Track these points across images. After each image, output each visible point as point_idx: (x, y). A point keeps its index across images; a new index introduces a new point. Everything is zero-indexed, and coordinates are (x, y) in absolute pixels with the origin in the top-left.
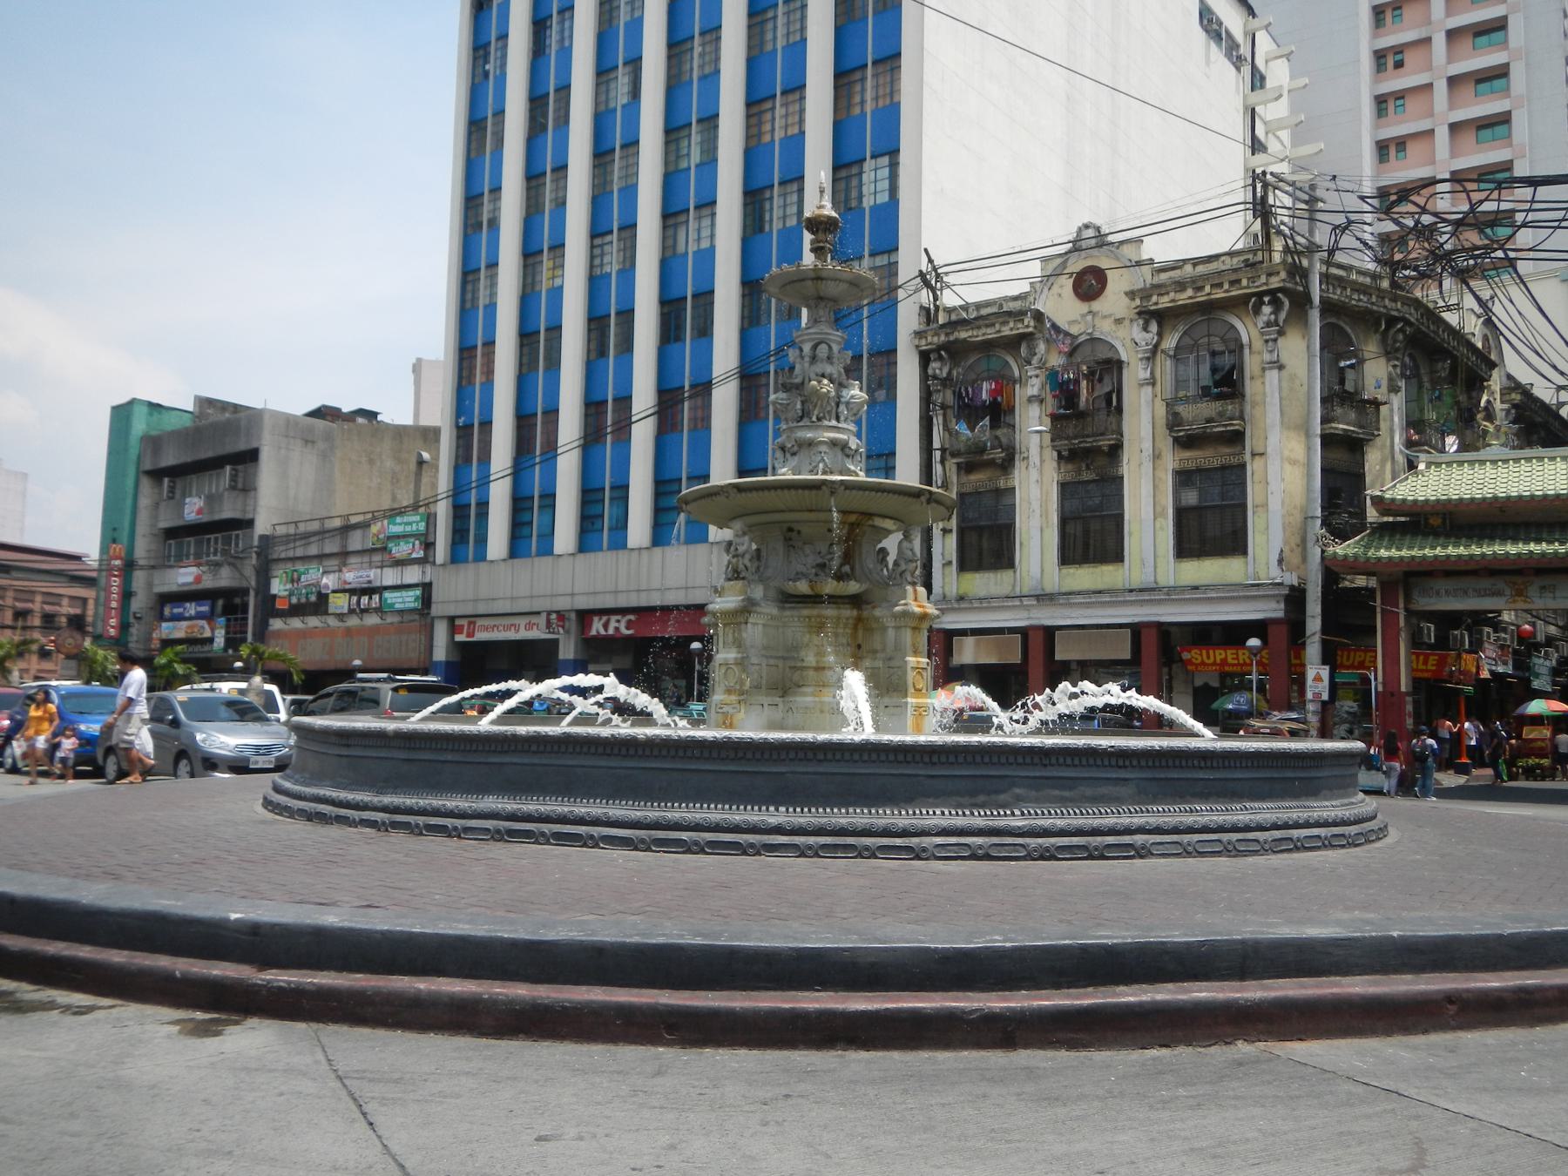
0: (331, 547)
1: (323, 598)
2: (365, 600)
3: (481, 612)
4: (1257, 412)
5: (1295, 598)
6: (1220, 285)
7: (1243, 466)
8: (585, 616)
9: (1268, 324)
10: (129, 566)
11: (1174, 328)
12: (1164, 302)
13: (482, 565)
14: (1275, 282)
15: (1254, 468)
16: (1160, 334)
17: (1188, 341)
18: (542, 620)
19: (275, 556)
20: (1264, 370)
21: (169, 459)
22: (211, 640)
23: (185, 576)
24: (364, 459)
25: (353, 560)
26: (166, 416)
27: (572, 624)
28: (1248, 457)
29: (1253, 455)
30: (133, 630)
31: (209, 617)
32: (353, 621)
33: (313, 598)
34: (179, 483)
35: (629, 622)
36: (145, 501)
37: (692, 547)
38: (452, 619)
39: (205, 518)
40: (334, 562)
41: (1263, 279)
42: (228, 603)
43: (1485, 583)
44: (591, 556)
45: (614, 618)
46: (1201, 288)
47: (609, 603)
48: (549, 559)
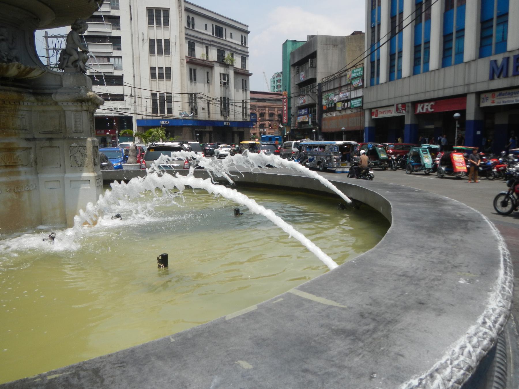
0: (337, 85)
1: (335, 104)
2: (346, 104)
3: (379, 105)
8: (415, 104)
10: (289, 98)
13: (379, 86)
18: (394, 109)
19: (324, 90)
21: (296, 60)
22: (308, 122)
23: (301, 101)
24: (358, 49)
25: (343, 89)
26: (298, 43)
27: (409, 108)
30: (292, 120)
31: (307, 114)
32: (344, 113)
33: (333, 105)
34: (300, 68)
35: (432, 105)
36: (292, 76)
37: (457, 66)
38: (370, 109)
39: (305, 79)
40: (337, 91)
42: (309, 107)
44: (416, 76)
45: (426, 104)
47: (422, 97)
48: (400, 80)
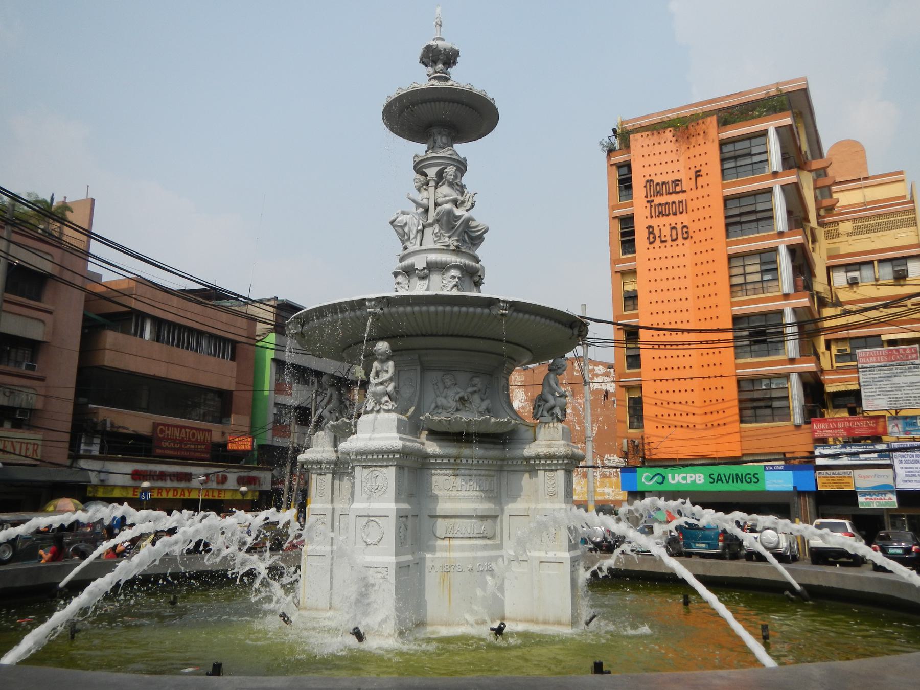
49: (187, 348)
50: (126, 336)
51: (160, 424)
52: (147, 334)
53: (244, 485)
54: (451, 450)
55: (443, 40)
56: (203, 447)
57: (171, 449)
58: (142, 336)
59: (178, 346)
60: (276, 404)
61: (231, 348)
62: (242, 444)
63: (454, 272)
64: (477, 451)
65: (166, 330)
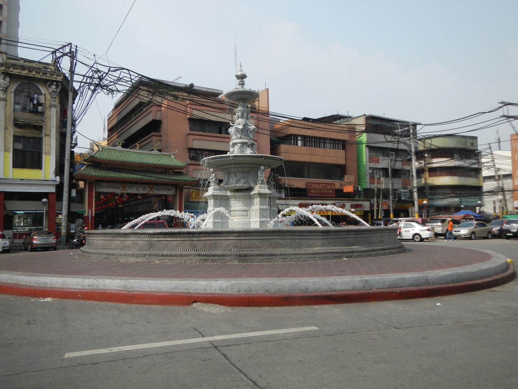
4: (47, 121)
5: (60, 187)
6: (39, 73)
7: (40, 140)
9: (54, 92)
11: (16, 82)
12: (16, 72)
14: (59, 79)
15: (45, 140)
16: (9, 82)
17: (20, 88)
20: (51, 107)
28: (43, 135)
29: (46, 135)
41: (55, 76)
43: (115, 185)
46: (31, 72)
49: (319, 147)
50: (290, 146)
51: (309, 183)
52: (299, 143)
53: (354, 208)
54: (233, 194)
55: (242, 71)
56: (331, 191)
57: (316, 193)
58: (297, 144)
59: (315, 146)
60: (370, 168)
61: (343, 144)
62: (349, 189)
63: (239, 145)
64: (240, 194)
65: (307, 140)
